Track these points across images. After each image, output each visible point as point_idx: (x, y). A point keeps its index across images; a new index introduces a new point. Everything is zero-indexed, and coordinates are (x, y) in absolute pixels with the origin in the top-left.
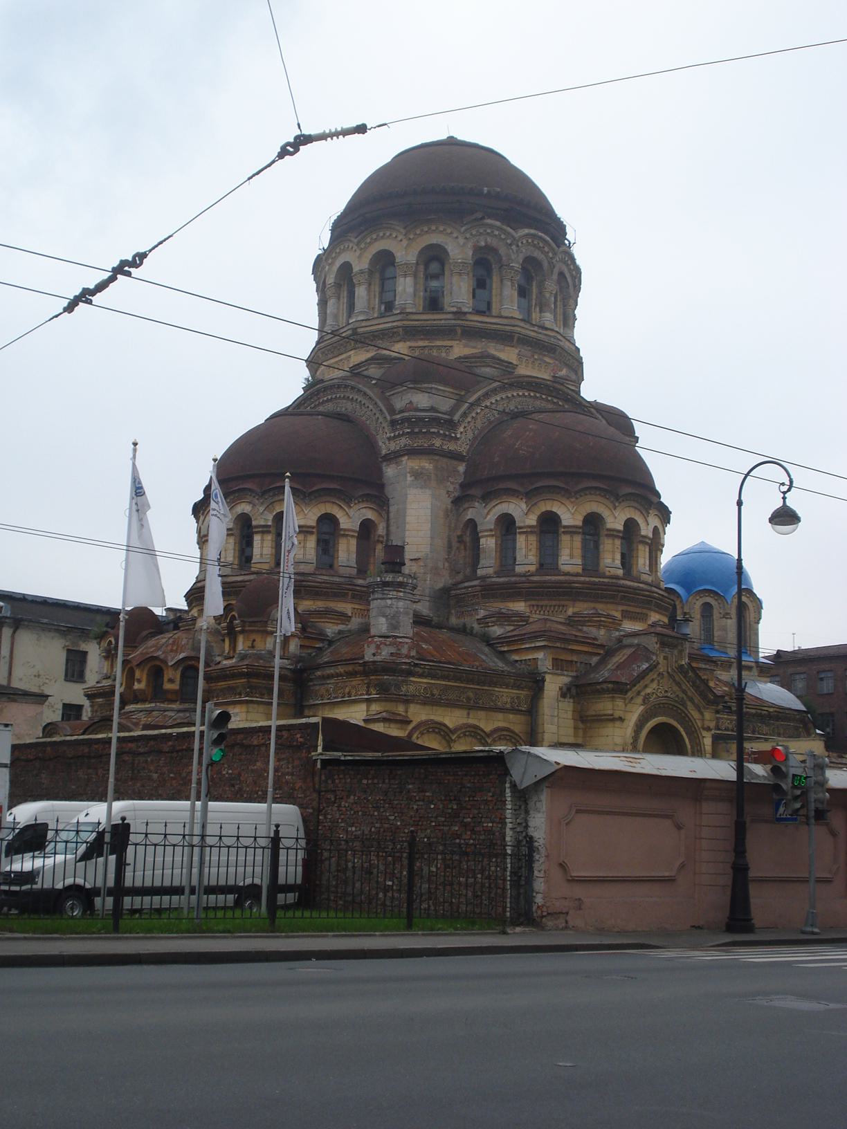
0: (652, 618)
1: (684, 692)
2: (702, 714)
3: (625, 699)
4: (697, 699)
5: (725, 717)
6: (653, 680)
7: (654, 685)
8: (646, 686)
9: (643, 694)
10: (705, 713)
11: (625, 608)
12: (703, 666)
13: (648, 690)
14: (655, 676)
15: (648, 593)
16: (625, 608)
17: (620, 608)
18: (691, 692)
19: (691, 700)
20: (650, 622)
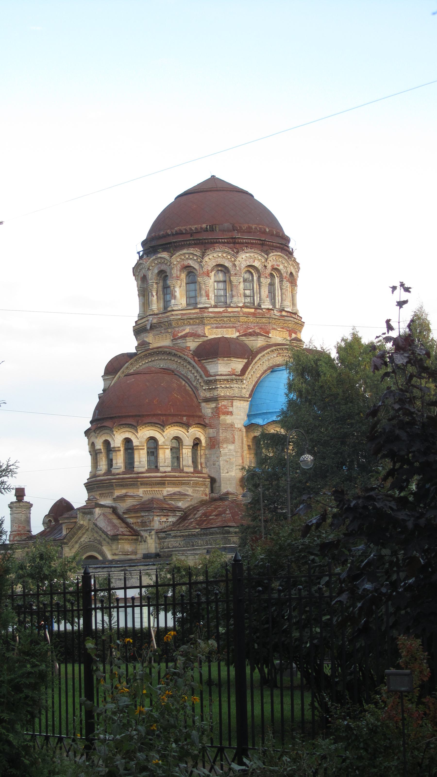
0: (116, 494)
1: (101, 536)
2: (111, 546)
3: (68, 547)
4: (107, 539)
5: (172, 540)
6: (83, 534)
7: (85, 536)
8: (80, 538)
9: (79, 542)
10: (113, 546)
11: (100, 492)
12: (144, 514)
13: (82, 540)
14: (84, 531)
15: (107, 481)
16: (100, 492)
17: (98, 493)
18: (104, 536)
19: (104, 540)
20: (115, 497)
